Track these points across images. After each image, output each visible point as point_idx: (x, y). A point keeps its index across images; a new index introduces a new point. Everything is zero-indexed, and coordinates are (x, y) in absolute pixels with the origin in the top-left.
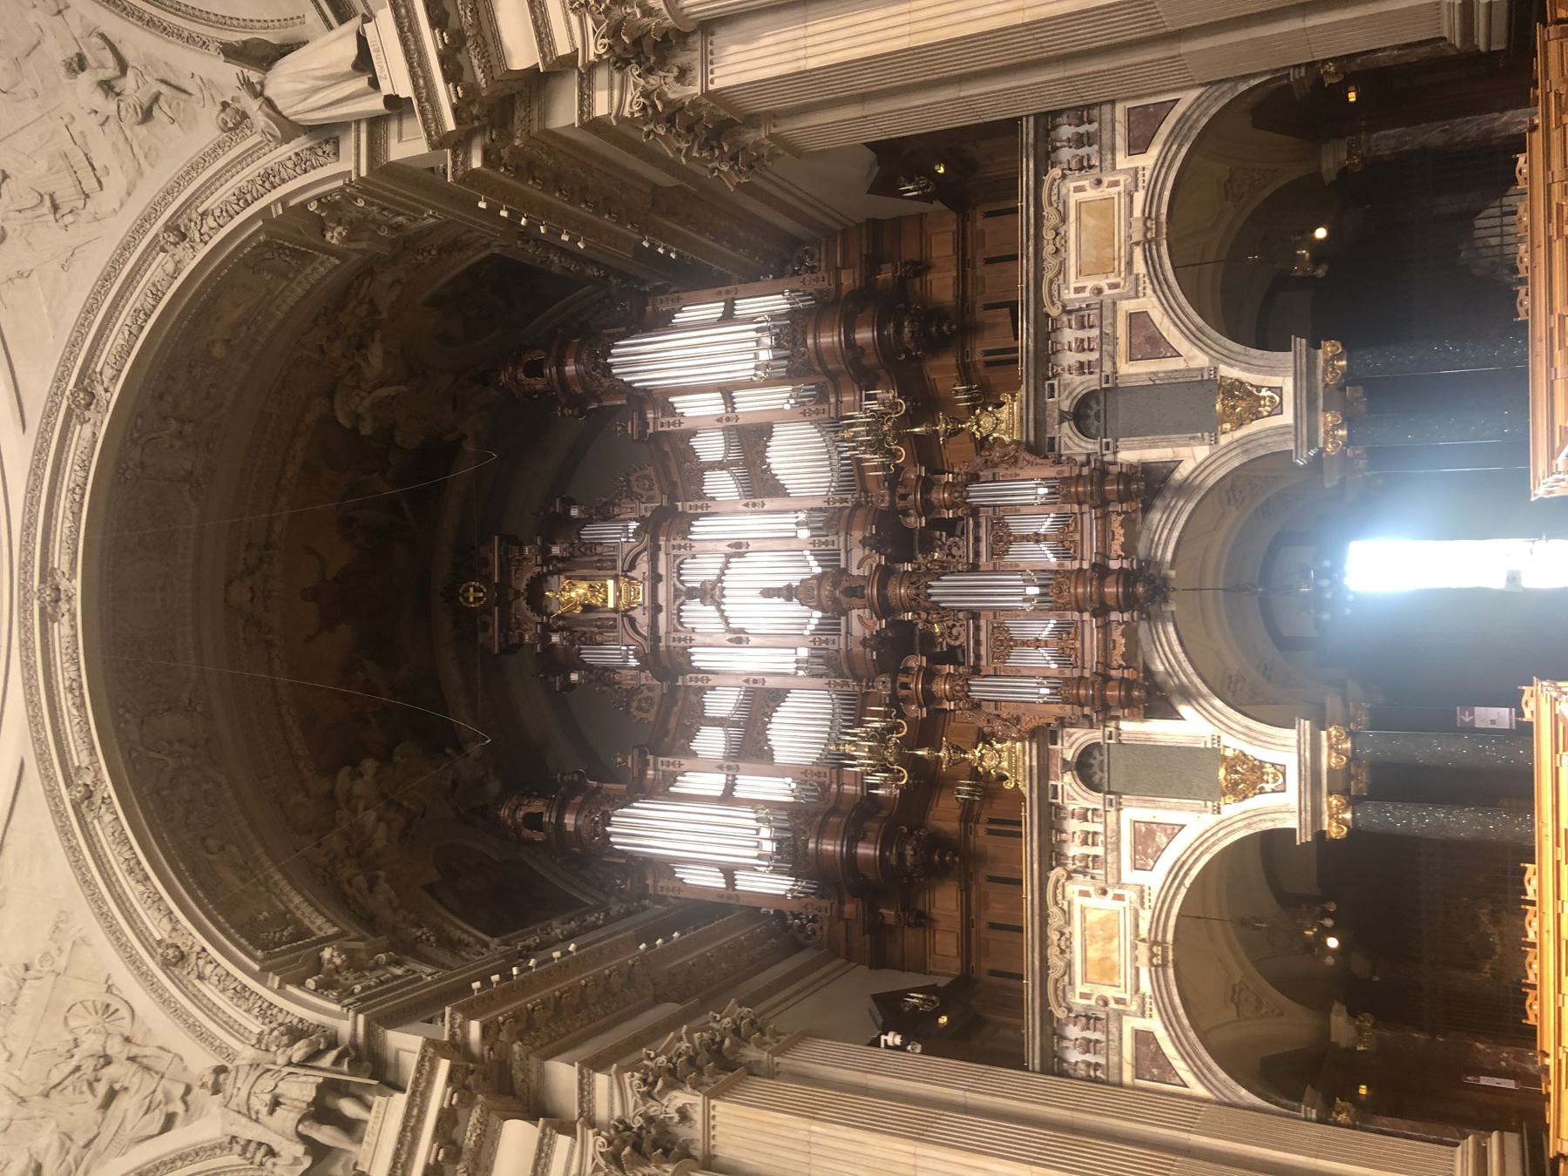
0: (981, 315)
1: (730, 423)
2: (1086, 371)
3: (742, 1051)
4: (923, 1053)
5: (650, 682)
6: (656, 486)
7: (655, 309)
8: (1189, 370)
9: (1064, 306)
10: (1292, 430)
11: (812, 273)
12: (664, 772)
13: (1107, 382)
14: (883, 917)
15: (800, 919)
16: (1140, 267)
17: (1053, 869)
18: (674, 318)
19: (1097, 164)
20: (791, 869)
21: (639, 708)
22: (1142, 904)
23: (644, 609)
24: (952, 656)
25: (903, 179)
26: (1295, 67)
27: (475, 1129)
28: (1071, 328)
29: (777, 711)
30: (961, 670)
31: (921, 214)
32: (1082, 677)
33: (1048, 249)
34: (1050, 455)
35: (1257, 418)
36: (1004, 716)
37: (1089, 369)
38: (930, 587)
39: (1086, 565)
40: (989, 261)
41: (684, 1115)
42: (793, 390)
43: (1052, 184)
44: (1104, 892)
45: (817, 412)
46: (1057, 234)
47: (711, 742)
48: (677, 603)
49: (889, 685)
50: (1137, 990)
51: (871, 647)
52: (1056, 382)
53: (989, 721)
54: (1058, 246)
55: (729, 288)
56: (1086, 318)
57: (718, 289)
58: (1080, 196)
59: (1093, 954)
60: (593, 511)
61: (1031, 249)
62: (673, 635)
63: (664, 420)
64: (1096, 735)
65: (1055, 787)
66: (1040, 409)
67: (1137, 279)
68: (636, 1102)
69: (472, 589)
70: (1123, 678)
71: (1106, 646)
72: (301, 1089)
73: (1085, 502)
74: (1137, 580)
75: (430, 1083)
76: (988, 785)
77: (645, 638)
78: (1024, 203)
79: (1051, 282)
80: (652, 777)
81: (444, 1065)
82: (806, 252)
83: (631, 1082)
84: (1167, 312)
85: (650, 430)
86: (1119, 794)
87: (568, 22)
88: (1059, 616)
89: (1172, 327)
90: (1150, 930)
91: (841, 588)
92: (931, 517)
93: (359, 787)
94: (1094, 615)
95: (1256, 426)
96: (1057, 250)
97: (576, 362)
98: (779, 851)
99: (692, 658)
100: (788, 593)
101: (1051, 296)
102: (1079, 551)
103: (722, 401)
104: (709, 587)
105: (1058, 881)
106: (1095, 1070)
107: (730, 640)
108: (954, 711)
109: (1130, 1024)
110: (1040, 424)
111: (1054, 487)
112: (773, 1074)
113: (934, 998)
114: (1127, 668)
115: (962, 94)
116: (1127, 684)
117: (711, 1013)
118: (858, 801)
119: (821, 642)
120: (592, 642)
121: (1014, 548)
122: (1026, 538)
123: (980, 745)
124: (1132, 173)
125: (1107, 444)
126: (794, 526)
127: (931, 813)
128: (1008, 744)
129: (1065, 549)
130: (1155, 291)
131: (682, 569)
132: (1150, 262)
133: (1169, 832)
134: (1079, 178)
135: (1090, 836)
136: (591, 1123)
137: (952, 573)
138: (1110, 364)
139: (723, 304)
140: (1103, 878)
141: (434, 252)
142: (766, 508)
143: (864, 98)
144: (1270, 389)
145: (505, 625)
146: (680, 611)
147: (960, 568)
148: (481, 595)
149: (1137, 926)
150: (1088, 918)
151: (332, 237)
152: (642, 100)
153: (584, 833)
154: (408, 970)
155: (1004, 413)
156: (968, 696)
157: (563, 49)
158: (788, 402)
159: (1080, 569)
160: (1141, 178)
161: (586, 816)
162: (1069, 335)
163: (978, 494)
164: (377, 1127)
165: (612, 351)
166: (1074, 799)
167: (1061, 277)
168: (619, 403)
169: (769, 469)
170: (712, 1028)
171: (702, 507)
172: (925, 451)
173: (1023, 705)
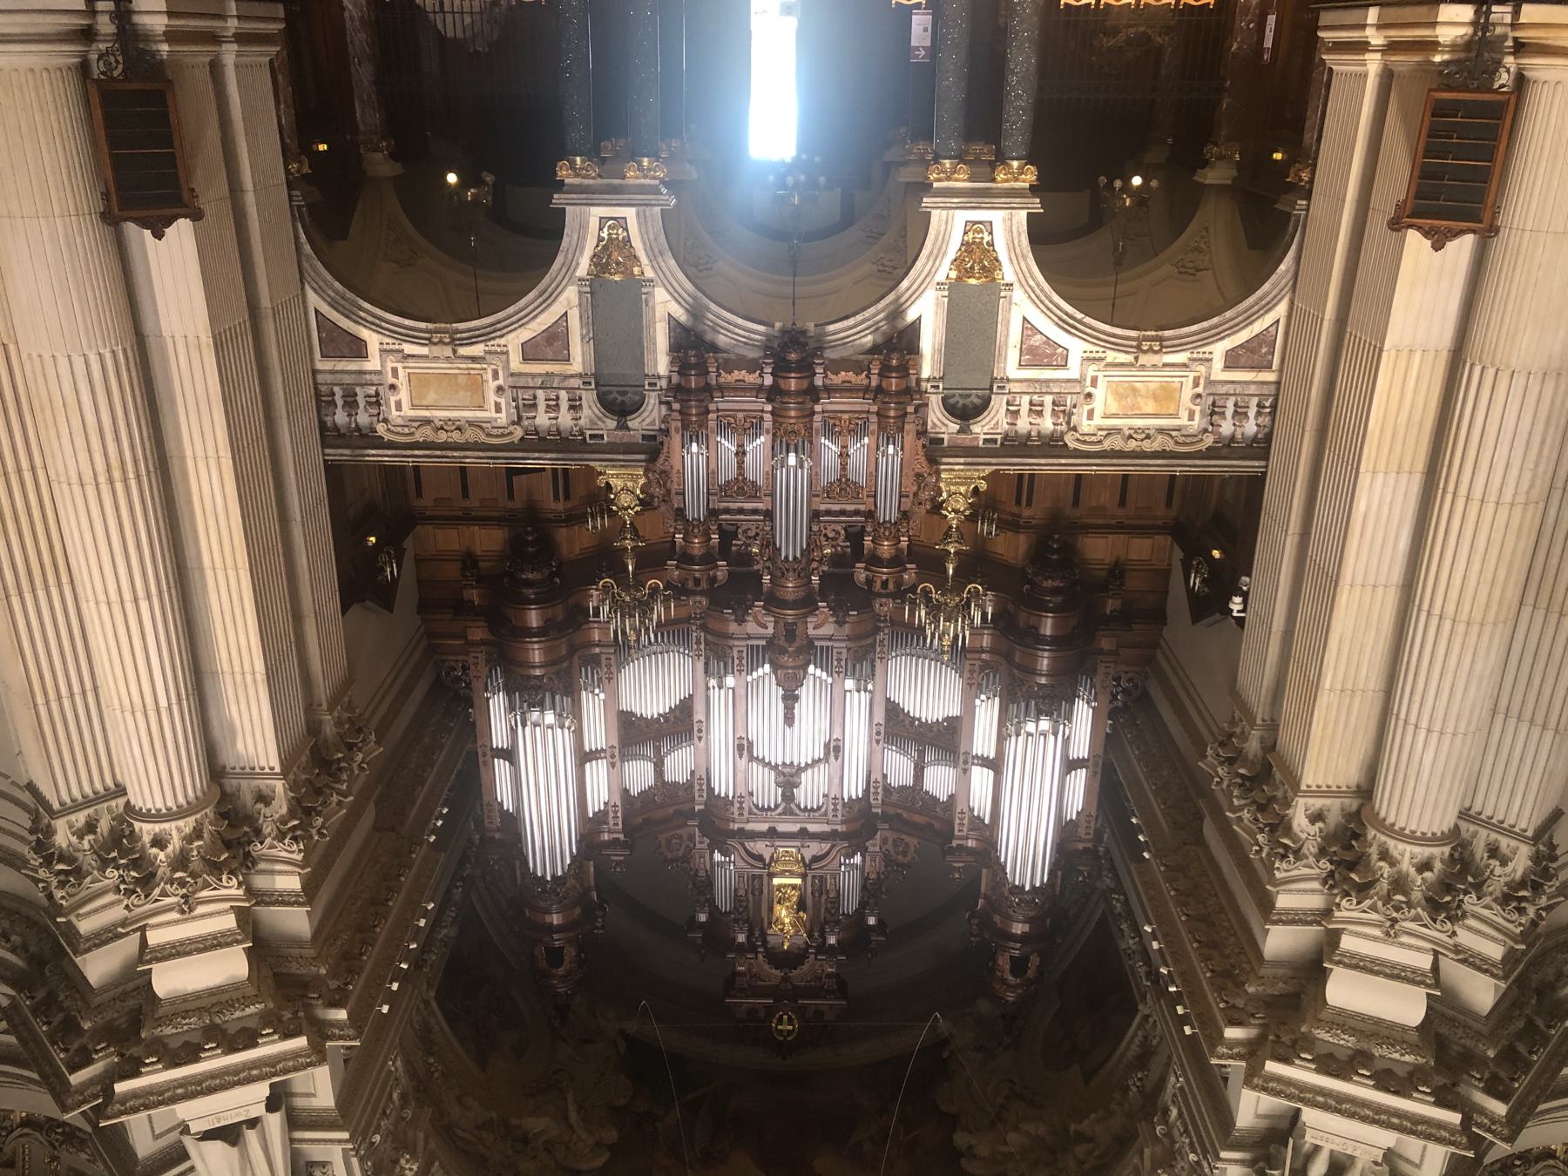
0: (518, 503)
1: (617, 754)
2: (578, 403)
3: (1251, 756)
4: (1249, 575)
5: (878, 842)
6: (678, 832)
7: (498, 830)
8: (580, 305)
9: (514, 423)
10: (641, 208)
11: (469, 668)
12: (970, 830)
13: (590, 383)
14: (1115, 611)
15: (1118, 693)
16: (478, 350)
17: (1066, 444)
18: (508, 810)
19: (374, 388)
20: (1067, 702)
21: (905, 853)
22: (1101, 359)
23: (803, 846)
24: (855, 537)
25: (380, 578)
26: (291, 200)
27: (1337, 1035)
28: (535, 417)
30: (869, 529)
31: (416, 560)
32: (878, 414)
33: (456, 437)
34: (659, 439)
35: (629, 241)
36: (915, 488)
37: (575, 400)
38: (787, 557)
39: (769, 408)
40: (465, 494)
41: (1316, 817)
42: (586, 690)
43: (393, 432)
44: (1089, 395)
45: (609, 666)
46: (442, 428)
47: (939, 780)
48: (798, 812)
49: (884, 600)
50: (1185, 365)
51: (844, 616)
52: (588, 432)
53: (920, 504)
54: (453, 428)
55: (480, 753)
56: (526, 402)
57: (481, 764)
58: (405, 405)
59: (1150, 407)
60: (702, 898)
61: (455, 454)
62: (830, 814)
63: (611, 822)
64: (935, 401)
65: (986, 441)
66: (614, 448)
67: (490, 352)
68: (1305, 866)
69: (780, 1027)
70: (879, 374)
71: (847, 390)
73: (707, 407)
74: (784, 359)
75: (1290, 1082)
76: (983, 505)
77: (833, 847)
78: (410, 460)
79: (488, 435)
80: (974, 842)
81: (1271, 1067)
82: (448, 674)
83: (1286, 871)
84: (523, 325)
85: (621, 836)
86: (993, 380)
87: (203, 916)
88: (817, 434)
89: (538, 320)
90: (1126, 352)
91: (786, 645)
92: (718, 557)
93: (983, 1151)
94: (817, 401)
95: (637, 243)
96: (458, 429)
97: (550, 913)
98: (1049, 714)
99: (854, 797)
100: (790, 699)
101: (503, 435)
102: (754, 414)
103: (594, 762)
104: (781, 779)
105: (1078, 440)
106: (1264, 407)
107: (836, 758)
108: (909, 537)
109: (1218, 372)
110: (629, 449)
111: (691, 436)
112: (1273, 726)
113: (1195, 563)
114: (869, 370)
115: (299, 519)
116: (885, 371)
117: (1213, 787)
118: (998, 633)
119: (839, 666)
121: (750, 476)
122: (741, 464)
123: (944, 512)
124: (384, 356)
125: (650, 384)
126: (722, 691)
128: (942, 485)
129: (752, 427)
130: (502, 336)
131: (763, 806)
132: (474, 340)
133: (1030, 333)
134: (388, 405)
135: (1034, 408)
136: (1326, 913)
137: (774, 537)
138: (572, 380)
139: (496, 760)
140: (1075, 396)
141: (431, 1060)
142: (703, 719)
143: (297, 617)
144: (601, 229)
147: (768, 528)
148: (785, 1017)
149: (1122, 365)
150: (1114, 412)
151: (411, 1169)
152: (286, 841)
153: (1032, 914)
154: (1173, 1102)
155: (617, 483)
156: (896, 523)
157: (230, 922)
158: (598, 695)
159: (772, 413)
160: (391, 347)
162: (542, 419)
163: (695, 509)
164: (1337, 1140)
166: (997, 422)
167: (484, 425)
168: (592, 869)
169: (664, 716)
170: (1228, 786)
171: (701, 785)
172: (652, 559)
173: (904, 471)
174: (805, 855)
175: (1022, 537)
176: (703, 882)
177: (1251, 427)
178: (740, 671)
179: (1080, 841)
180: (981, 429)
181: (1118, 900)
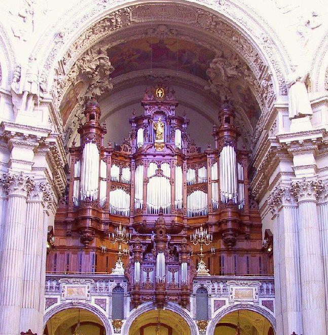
0: (233, 255)
16: (236, 303)
21: (125, 147)
44: (89, 292)
47: (115, 171)
59: (74, 289)
66: (205, 279)
71: (147, 294)
72: (35, 90)
81: (46, 135)
98: (87, 197)
109: (58, 297)
121: (171, 274)
145: (150, 104)
162: (221, 286)
165: (231, 147)
177: (49, 284)
180: (114, 284)
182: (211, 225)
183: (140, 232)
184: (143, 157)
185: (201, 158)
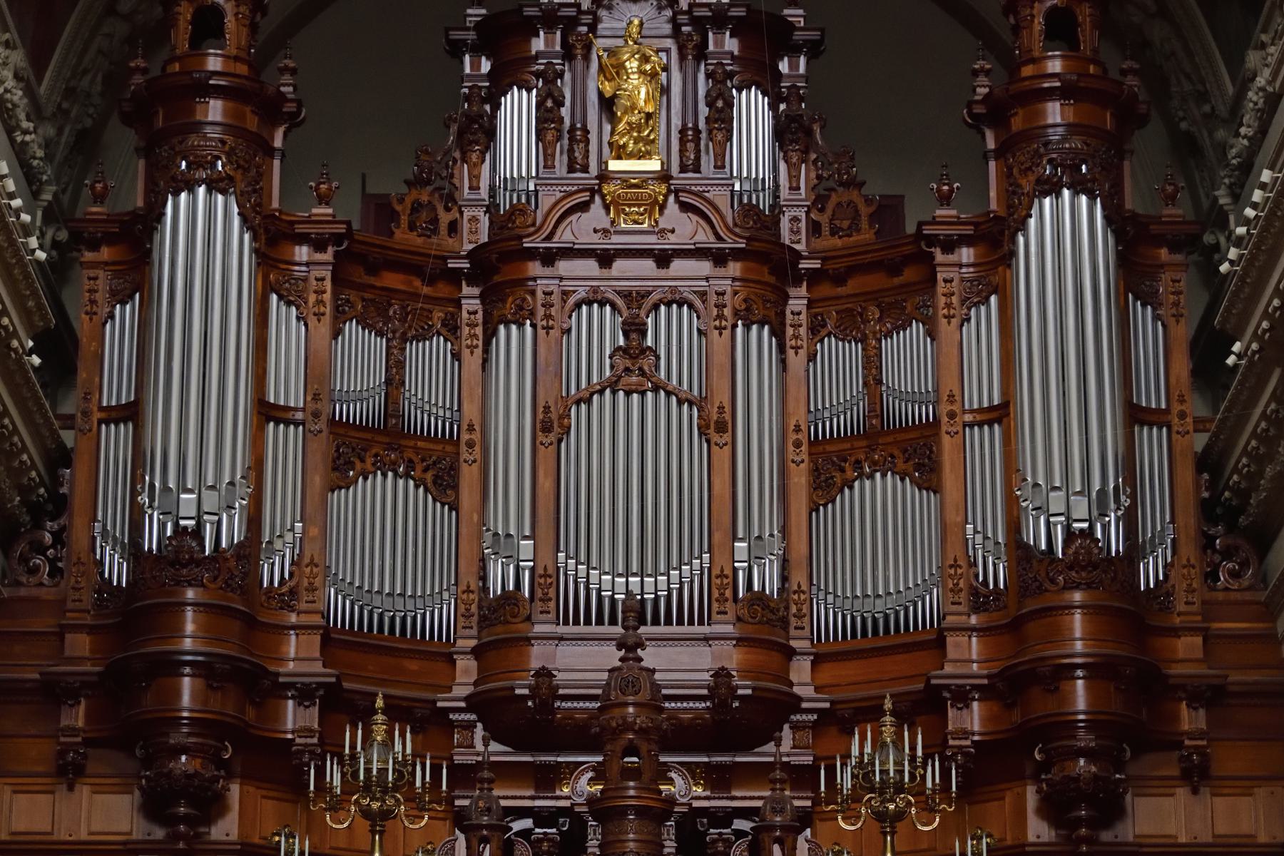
11: (1207, 576)
12: (305, 280)
14: (72, 706)
15: (53, 546)
18: (1144, 305)
21: (417, 207)
23: (605, 231)
29: (417, 487)
42: (997, 543)
48: (620, 302)
62: (556, 298)
77: (549, 238)
82: (1244, 565)
85: (940, 257)
98: (180, 531)
103: (986, 405)
104: (647, 363)
107: (547, 409)
118: (272, 668)
120: (547, 118)
127: (252, 789)
131: (680, 306)
139: (1163, 406)
146: (602, 304)
153: (194, 140)
158: (976, 532)
161: (223, 142)
165: (1084, 199)
174: (603, 212)
175: (234, 836)
176: (792, 142)
178: (722, 575)
179: (106, 264)
181: (26, 132)
182: (962, 697)
183: (519, 748)
184: (535, 268)
185: (895, 270)
